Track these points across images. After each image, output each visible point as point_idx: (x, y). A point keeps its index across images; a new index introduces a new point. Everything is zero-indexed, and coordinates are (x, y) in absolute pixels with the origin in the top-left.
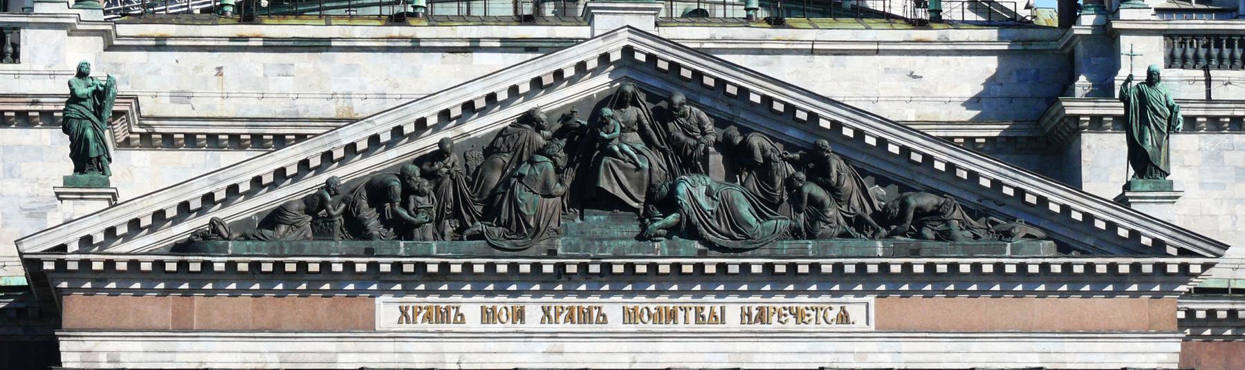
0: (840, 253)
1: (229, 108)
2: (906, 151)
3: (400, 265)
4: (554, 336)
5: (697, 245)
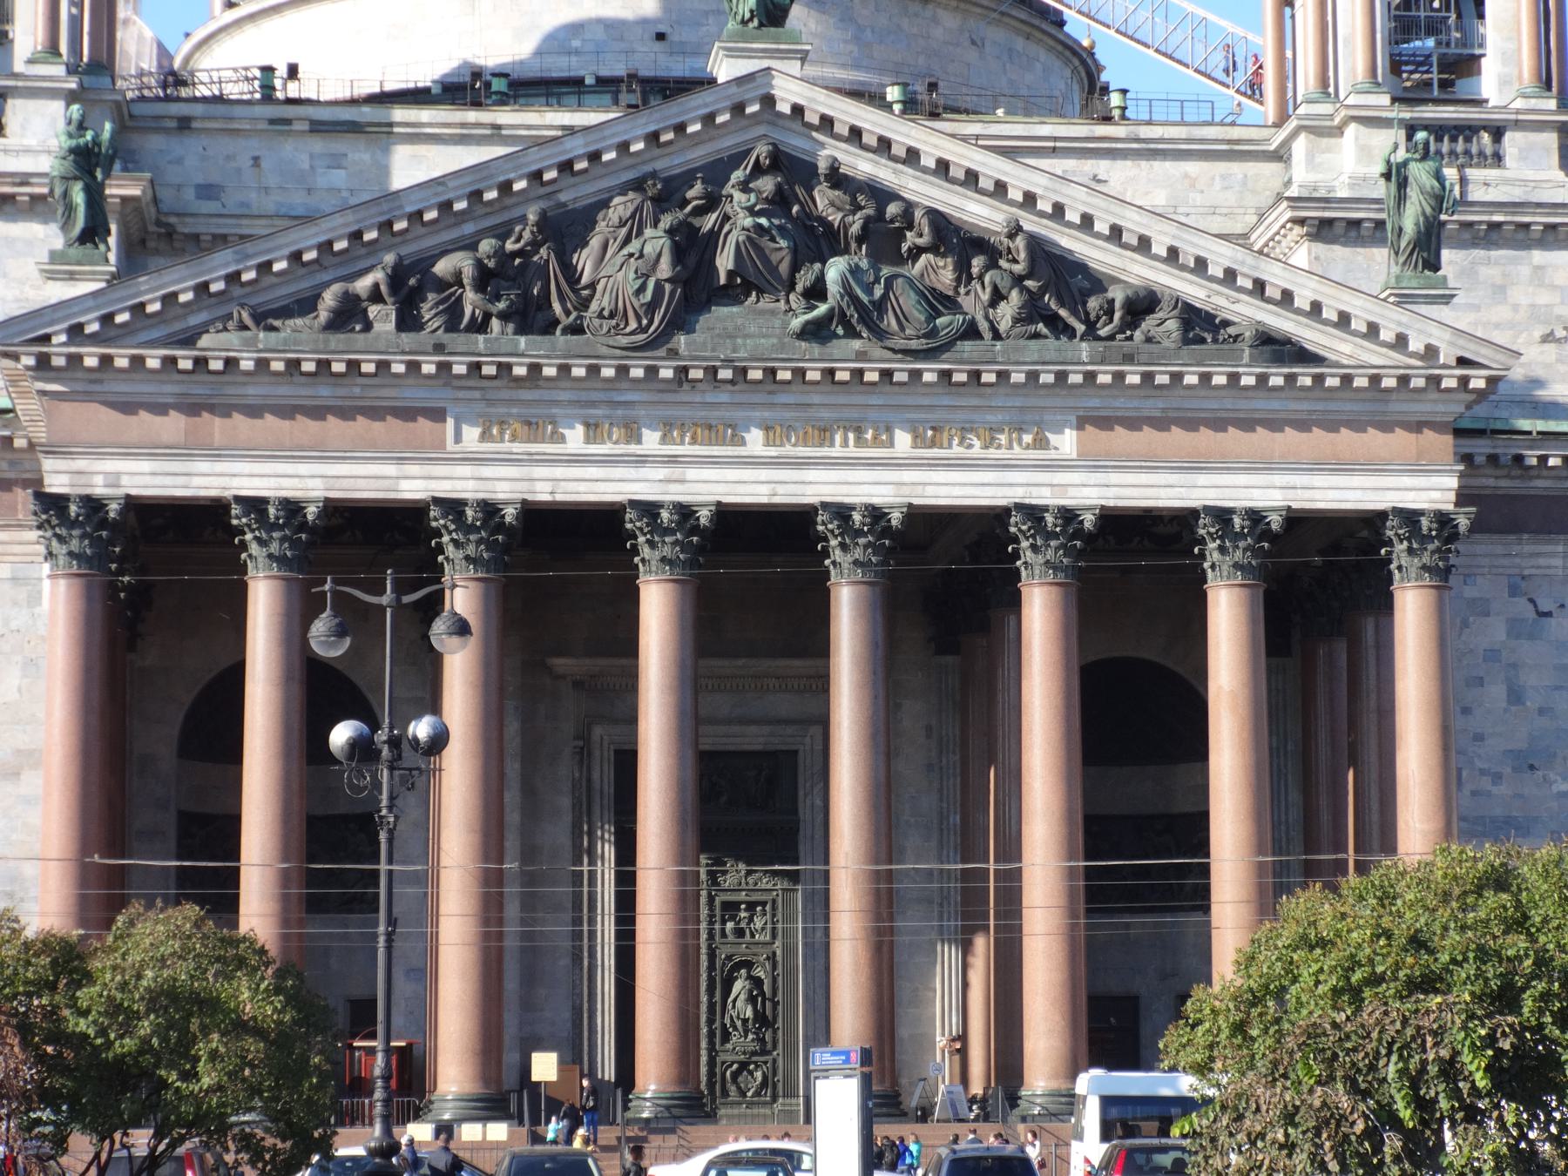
0: (1036, 357)
1: (269, 204)
3: (478, 366)
4: (673, 460)
5: (856, 344)
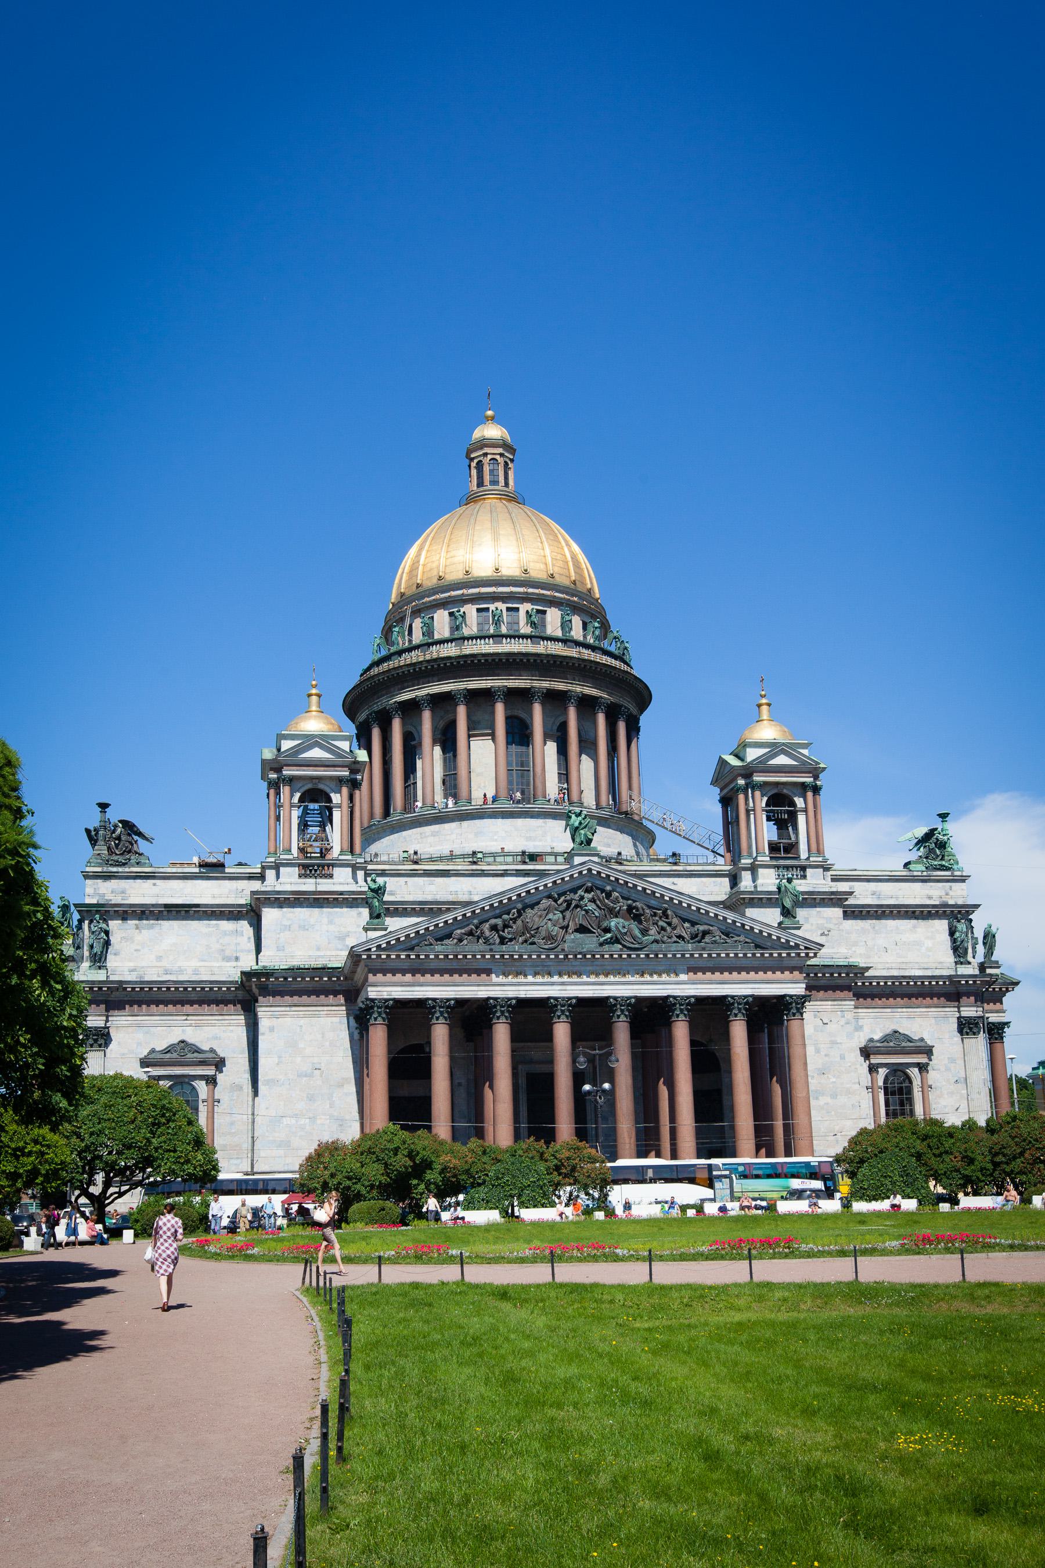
2: (699, 909)
4: (563, 984)
